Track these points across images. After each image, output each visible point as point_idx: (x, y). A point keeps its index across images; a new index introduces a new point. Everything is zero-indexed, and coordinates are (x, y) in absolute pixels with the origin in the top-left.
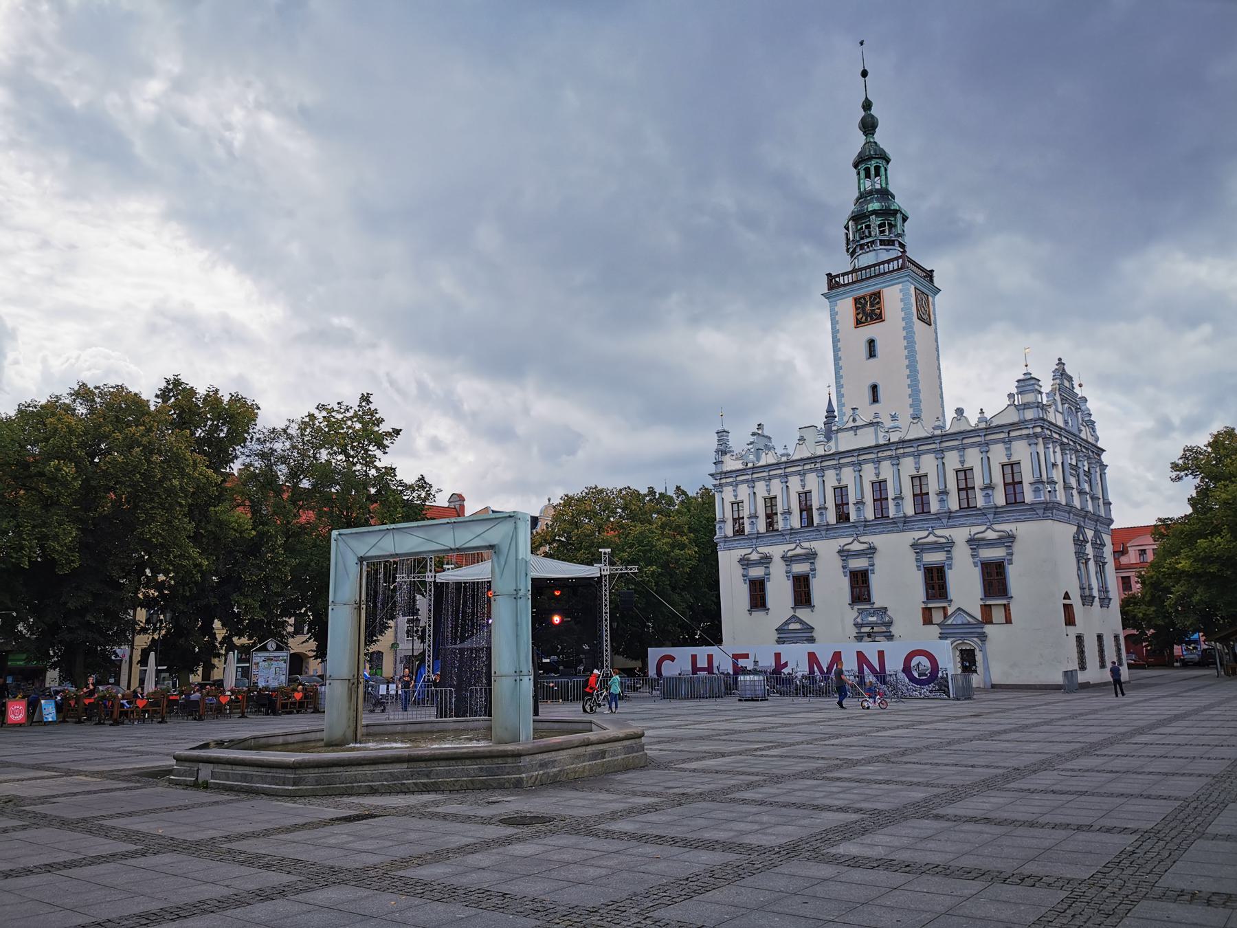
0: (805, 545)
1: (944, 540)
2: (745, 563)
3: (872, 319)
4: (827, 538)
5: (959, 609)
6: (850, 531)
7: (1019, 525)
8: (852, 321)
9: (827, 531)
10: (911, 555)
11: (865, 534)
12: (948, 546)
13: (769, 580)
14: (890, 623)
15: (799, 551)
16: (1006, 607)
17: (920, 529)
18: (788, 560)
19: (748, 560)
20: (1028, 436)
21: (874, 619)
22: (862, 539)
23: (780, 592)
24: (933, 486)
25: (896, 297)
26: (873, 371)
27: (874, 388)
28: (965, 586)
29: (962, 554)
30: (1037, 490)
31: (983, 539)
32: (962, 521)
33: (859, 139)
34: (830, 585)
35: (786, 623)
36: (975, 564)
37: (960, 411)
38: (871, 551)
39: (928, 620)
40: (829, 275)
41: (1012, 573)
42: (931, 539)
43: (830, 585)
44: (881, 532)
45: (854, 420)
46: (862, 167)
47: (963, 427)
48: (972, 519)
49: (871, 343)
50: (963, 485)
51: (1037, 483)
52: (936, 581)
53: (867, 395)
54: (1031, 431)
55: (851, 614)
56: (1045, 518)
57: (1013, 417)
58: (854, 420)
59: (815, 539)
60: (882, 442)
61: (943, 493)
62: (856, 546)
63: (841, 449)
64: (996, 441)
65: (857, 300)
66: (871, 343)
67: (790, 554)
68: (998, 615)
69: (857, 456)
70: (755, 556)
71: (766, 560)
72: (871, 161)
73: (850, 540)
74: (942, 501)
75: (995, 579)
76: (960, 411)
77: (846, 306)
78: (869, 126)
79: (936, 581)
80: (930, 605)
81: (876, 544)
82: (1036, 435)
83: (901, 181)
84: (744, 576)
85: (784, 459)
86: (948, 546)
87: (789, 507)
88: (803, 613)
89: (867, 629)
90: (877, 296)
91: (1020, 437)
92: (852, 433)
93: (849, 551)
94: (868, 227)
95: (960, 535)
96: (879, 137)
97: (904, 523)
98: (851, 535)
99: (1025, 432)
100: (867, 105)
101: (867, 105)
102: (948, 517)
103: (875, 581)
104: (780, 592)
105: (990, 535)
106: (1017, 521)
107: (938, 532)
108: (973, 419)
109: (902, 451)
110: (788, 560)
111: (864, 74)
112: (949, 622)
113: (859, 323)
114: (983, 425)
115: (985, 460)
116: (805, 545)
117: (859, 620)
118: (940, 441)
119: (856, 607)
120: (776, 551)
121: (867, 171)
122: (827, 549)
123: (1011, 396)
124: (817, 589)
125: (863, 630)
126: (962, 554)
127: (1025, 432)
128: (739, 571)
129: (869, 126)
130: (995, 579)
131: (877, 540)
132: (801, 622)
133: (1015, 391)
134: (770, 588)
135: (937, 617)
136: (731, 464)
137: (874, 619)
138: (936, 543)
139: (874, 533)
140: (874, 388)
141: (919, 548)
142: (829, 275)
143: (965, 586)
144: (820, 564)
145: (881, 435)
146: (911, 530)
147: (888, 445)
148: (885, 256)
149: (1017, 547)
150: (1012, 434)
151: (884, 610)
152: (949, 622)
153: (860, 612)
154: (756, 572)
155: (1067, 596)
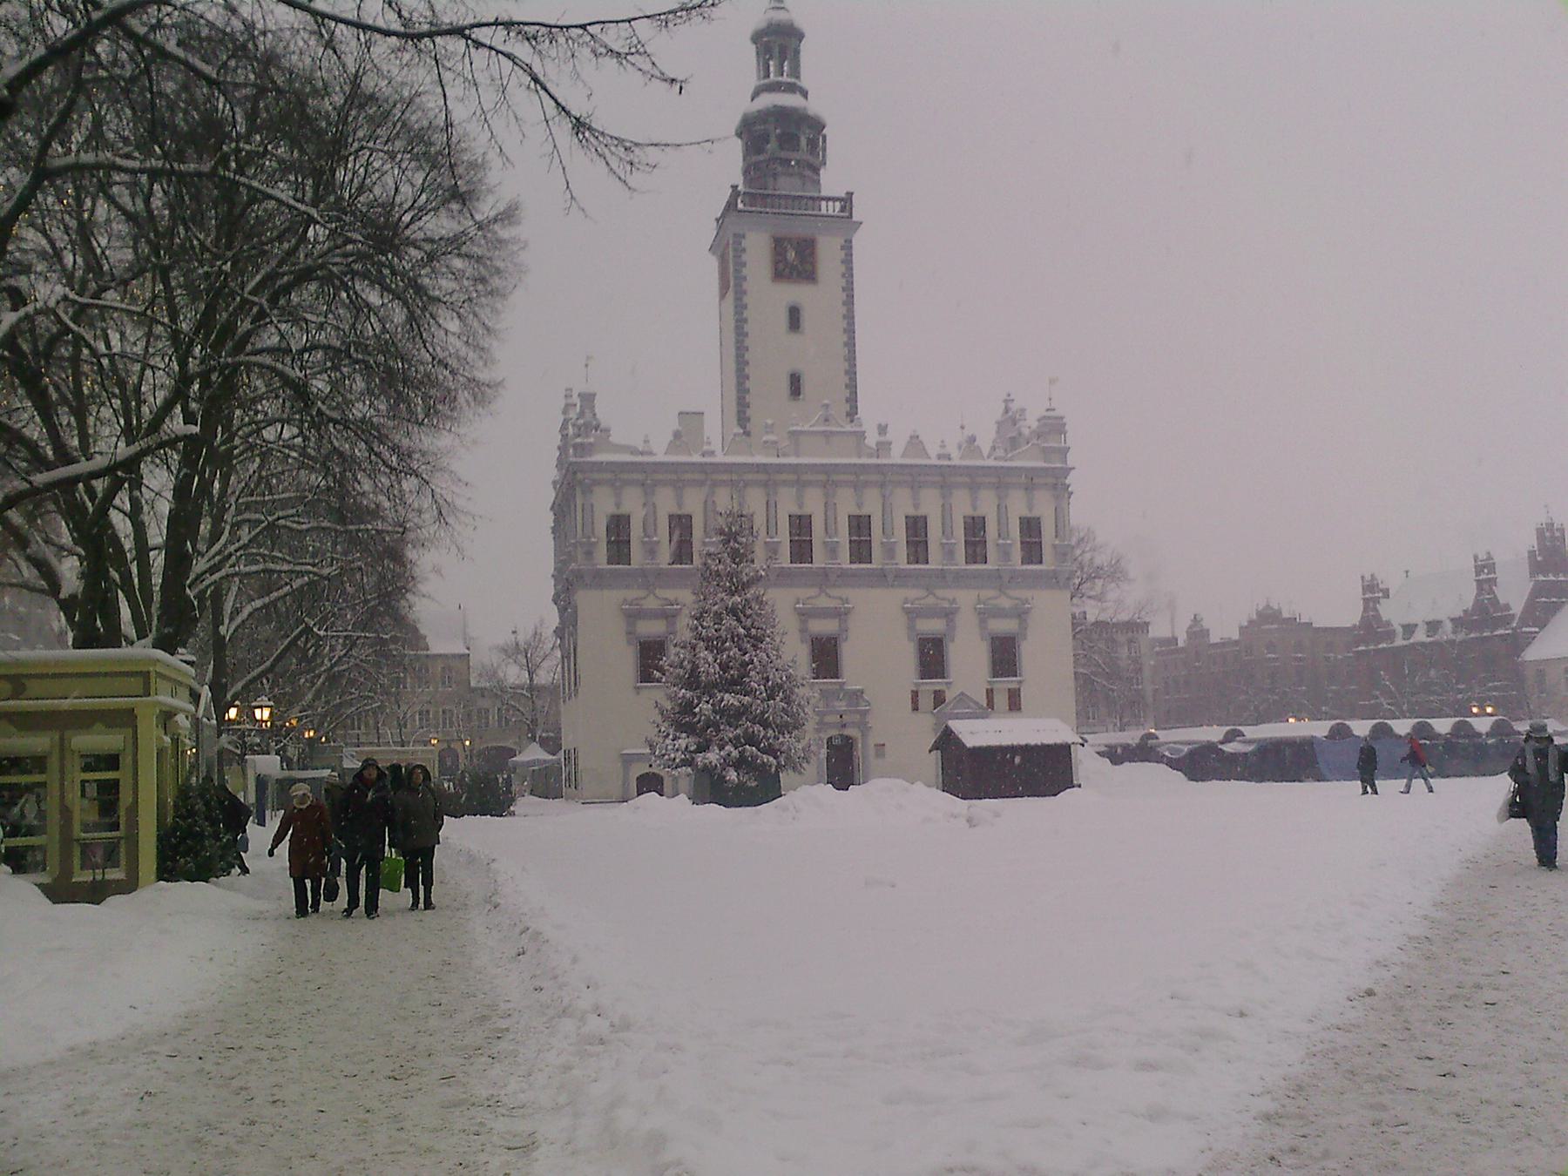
3: (799, 274)
11: (834, 586)
14: (864, 714)
22: (835, 592)
28: (968, 663)
38: (841, 614)
39: (915, 708)
42: (931, 600)
52: (932, 658)
62: (823, 602)
69: (829, 477)
70: (651, 603)
75: (1004, 656)
77: (758, 248)
79: (932, 658)
86: (949, 615)
89: (835, 719)
95: (965, 599)
105: (1005, 603)
107: (940, 593)
125: (829, 719)
130: (1004, 656)
143: (968, 663)
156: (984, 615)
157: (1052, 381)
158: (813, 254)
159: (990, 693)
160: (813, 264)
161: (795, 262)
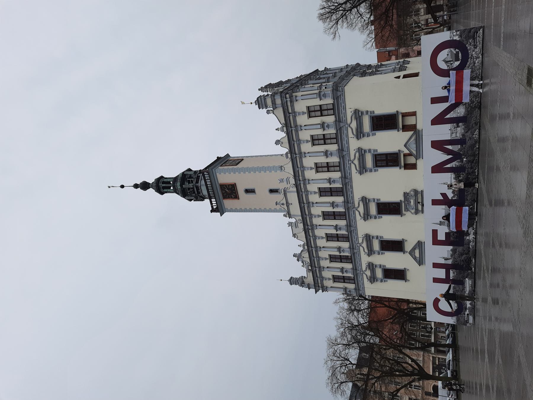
0: (360, 240)
1: (357, 155)
2: (373, 279)
4: (356, 227)
5: (405, 146)
6: (351, 213)
7: (347, 107)
8: (235, 201)
9: (351, 227)
10: (367, 176)
12: (361, 152)
13: (384, 266)
15: (364, 245)
16: (404, 115)
17: (350, 168)
18: (371, 252)
19: (371, 277)
20: (291, 102)
21: (412, 201)
22: (357, 205)
23: (393, 260)
24: (322, 160)
25: (224, 177)
26: (262, 192)
27: (272, 191)
28: (390, 141)
29: (367, 143)
30: (325, 96)
31: (357, 129)
32: (344, 142)
33: (151, 191)
34: (388, 227)
35: (415, 258)
36: (374, 135)
37: (278, 142)
38: (365, 201)
39: (413, 167)
40: (212, 211)
41: (379, 111)
42: (356, 162)
43: (388, 227)
44: (352, 192)
45: (283, 204)
46: (162, 190)
47: (286, 140)
48: (344, 136)
49: (247, 191)
50: (322, 142)
51: (320, 96)
52: (388, 160)
53: (274, 195)
54: (288, 100)
55: (409, 216)
56: (343, 91)
57: (280, 111)
58: (283, 204)
59: (357, 234)
60: (295, 189)
61: (326, 154)
63: (300, 214)
64: (295, 121)
65: (225, 197)
66: (247, 191)
67: (366, 250)
68: (410, 121)
70: (368, 273)
71: (371, 267)
72: (162, 185)
73: (357, 213)
74: (331, 154)
75: (384, 122)
76: (278, 142)
77: (228, 203)
78: (145, 186)
79: (388, 160)
80: (403, 164)
81: (360, 196)
82: (291, 97)
83: (172, 171)
84: (382, 281)
85: (306, 247)
86: (361, 152)
87: (336, 248)
88: (408, 247)
90: (223, 186)
91: (293, 106)
92: (290, 206)
93: (364, 214)
94: (189, 189)
95: (354, 144)
96: (151, 181)
97: (346, 179)
98: (354, 213)
99: (289, 104)
100: (136, 186)
101: (136, 186)
102: (342, 152)
103: (386, 198)
104: (393, 260)
105: (354, 125)
106: (345, 108)
107: (352, 157)
108: (282, 135)
109: (301, 177)
110: (371, 252)
111: (122, 187)
112: (415, 152)
113: (236, 197)
114: (285, 128)
115: (306, 128)
116: (360, 240)
117: (413, 211)
118: (295, 154)
119: (404, 212)
120: (365, 259)
121: (164, 188)
122: (363, 227)
123: (268, 112)
124: (390, 236)
126: (367, 143)
127: (289, 104)
128: (378, 284)
129: (145, 186)
130: (384, 122)
131: (357, 196)
132: (414, 249)
133: (265, 110)
134: (390, 265)
135: (411, 160)
136: (310, 279)
137: (412, 201)
138: (359, 159)
139: (353, 197)
140: (272, 191)
141: (363, 169)
142: (212, 211)
143: (390, 141)
144: (373, 232)
145: (291, 189)
146: (350, 174)
147: (297, 185)
148: (203, 182)
149: (363, 108)
150: (290, 111)
151: (406, 195)
152: (415, 152)
153: (407, 210)
154: (379, 273)
155: (398, 77)
156: (360, 134)
157: (243, 103)
158: (226, 185)
159: (406, 128)
160: (229, 185)
161: (230, 191)
